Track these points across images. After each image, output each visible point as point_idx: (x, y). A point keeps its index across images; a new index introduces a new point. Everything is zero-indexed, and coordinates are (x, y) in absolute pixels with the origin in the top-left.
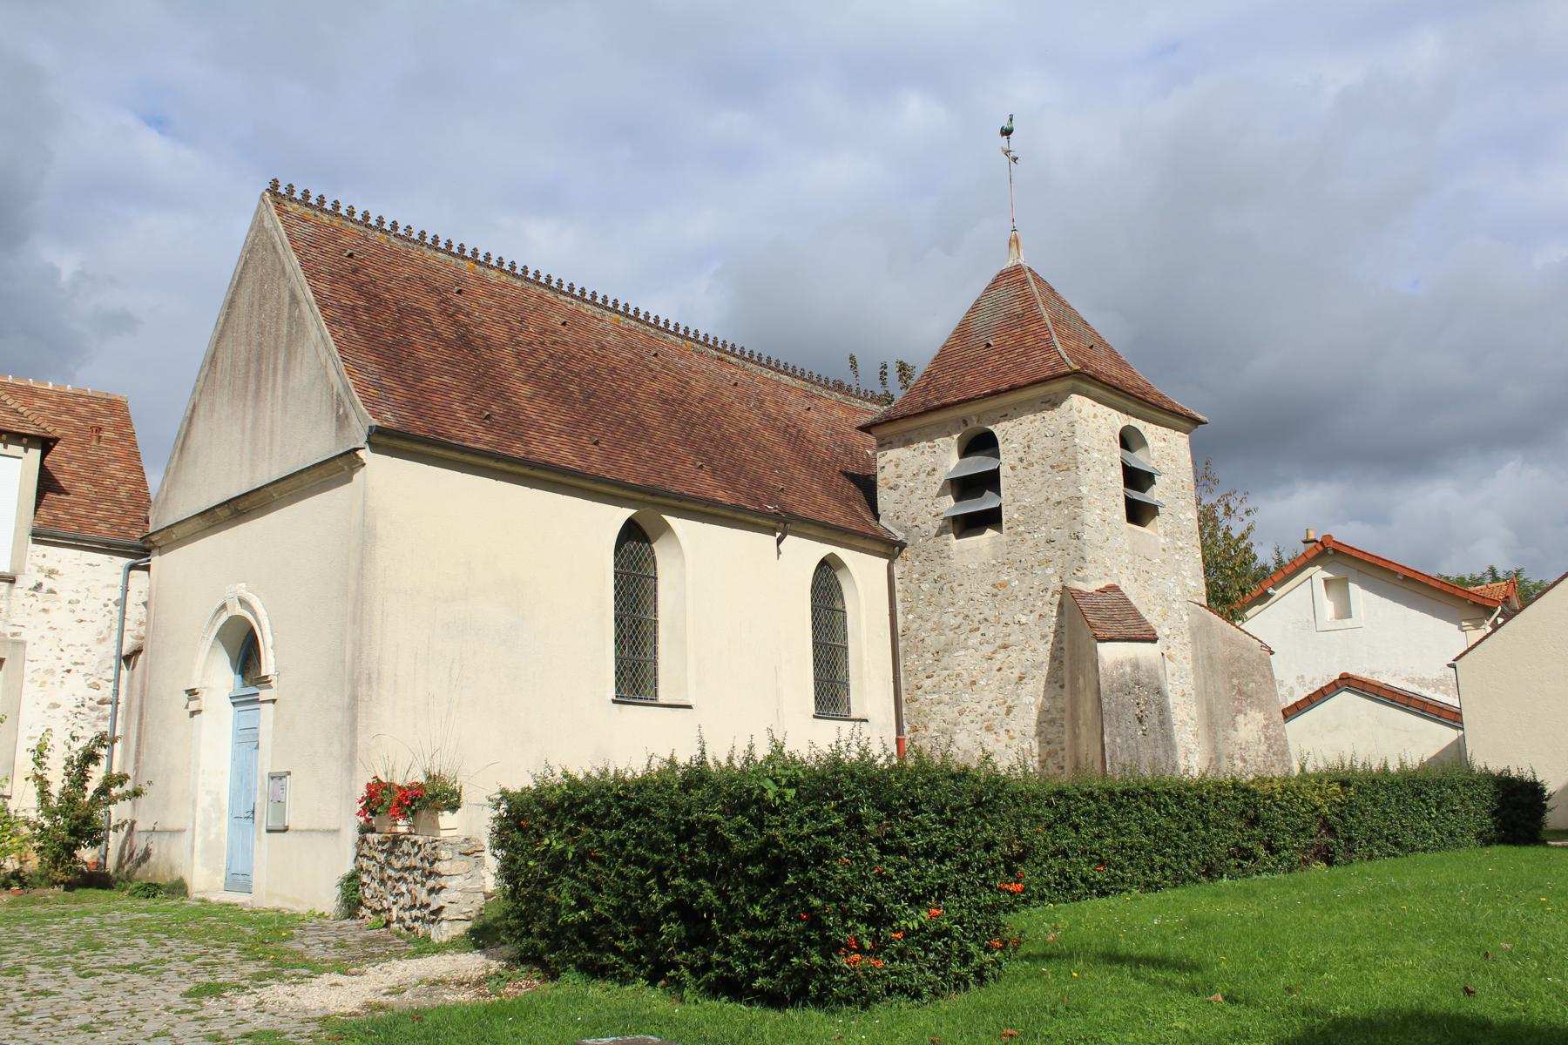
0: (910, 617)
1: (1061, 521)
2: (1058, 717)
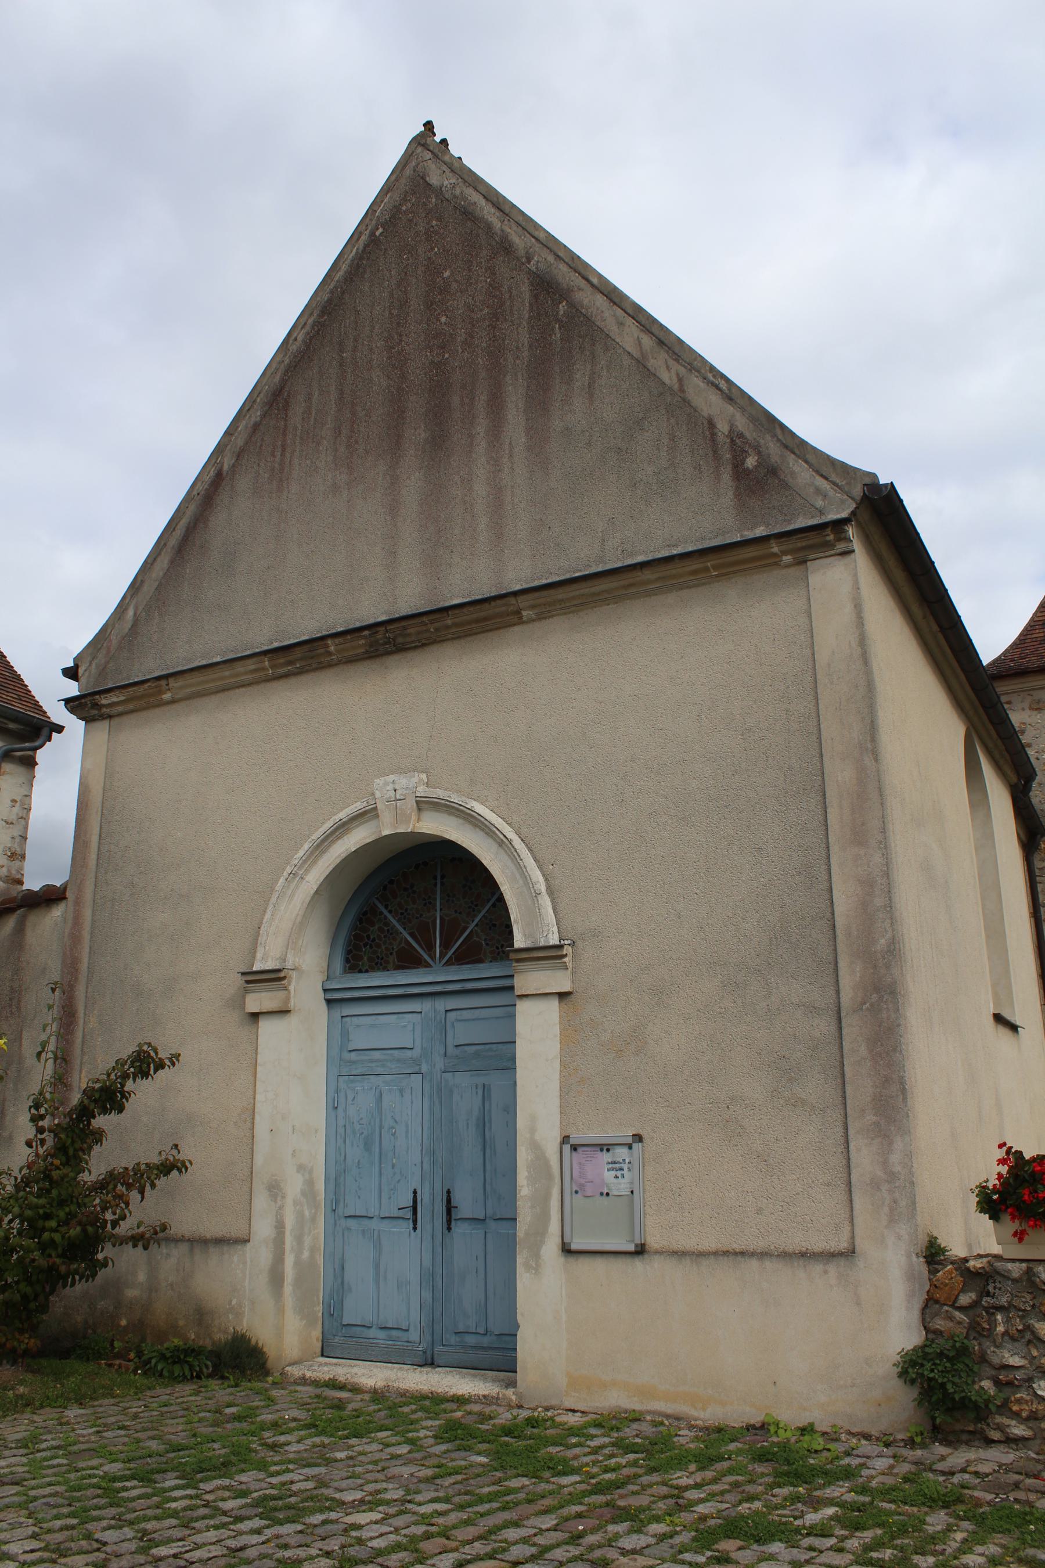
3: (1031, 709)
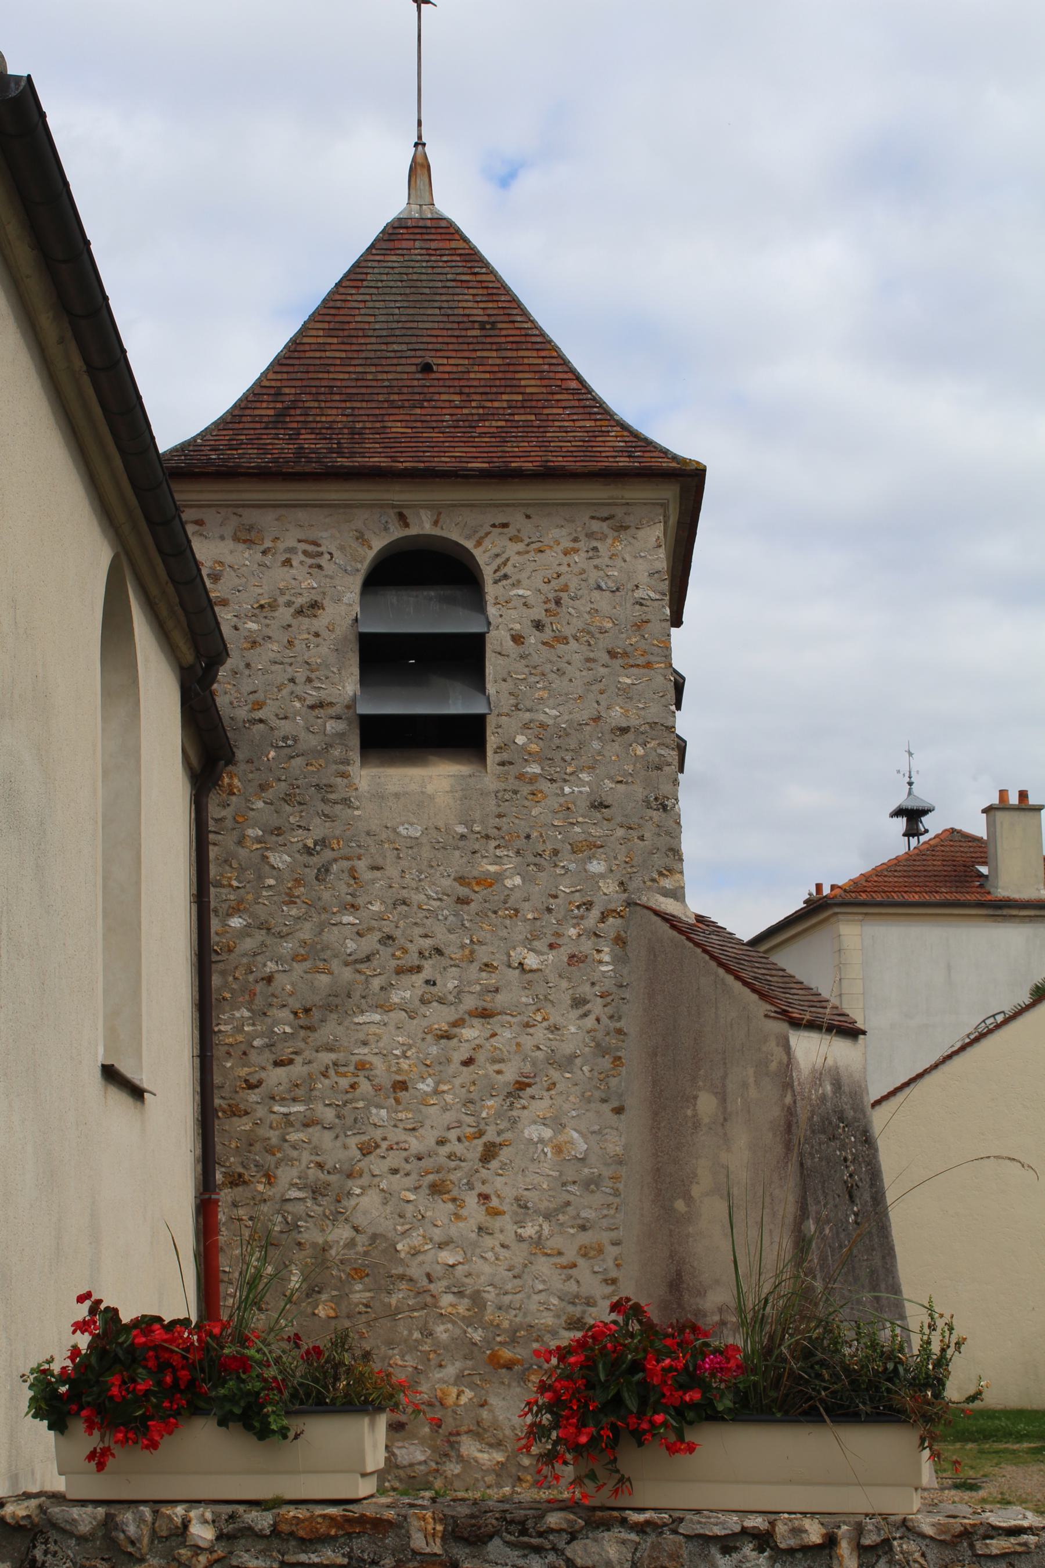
0: (236, 922)
1: (629, 768)
2: (607, 1173)
3: (236, 539)
